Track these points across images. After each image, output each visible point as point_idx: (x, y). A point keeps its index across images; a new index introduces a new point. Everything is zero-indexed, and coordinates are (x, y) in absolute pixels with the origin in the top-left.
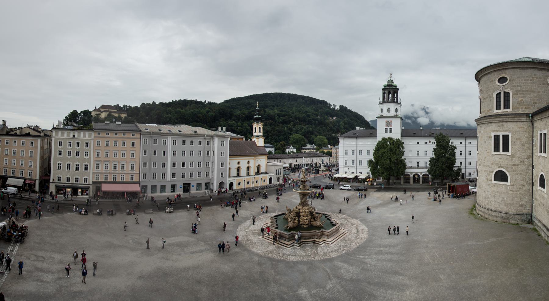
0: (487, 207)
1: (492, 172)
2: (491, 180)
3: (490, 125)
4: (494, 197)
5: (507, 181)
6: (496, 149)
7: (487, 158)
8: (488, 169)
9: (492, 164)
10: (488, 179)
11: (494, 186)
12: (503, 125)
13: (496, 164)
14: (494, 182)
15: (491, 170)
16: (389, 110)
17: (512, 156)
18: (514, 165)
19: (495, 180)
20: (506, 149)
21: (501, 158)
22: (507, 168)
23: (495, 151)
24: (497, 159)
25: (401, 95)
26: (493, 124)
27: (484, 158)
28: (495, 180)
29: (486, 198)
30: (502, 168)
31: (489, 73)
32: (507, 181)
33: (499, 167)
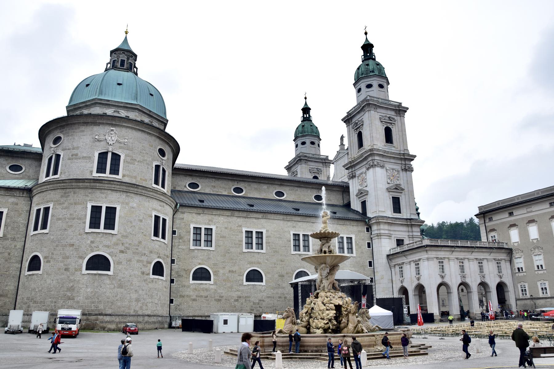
0: (140, 313)
1: (151, 263)
2: (148, 274)
3: (151, 200)
4: (152, 297)
5: (162, 275)
7: (143, 243)
8: (144, 258)
9: (151, 252)
10: (143, 273)
11: (153, 281)
12: (163, 207)
13: (155, 252)
14: (152, 276)
15: (149, 260)
19: (153, 274)
23: (154, 236)
24: (156, 246)
26: (154, 200)
27: (137, 243)
28: (153, 274)
29: (137, 300)
31: (150, 134)
32: (162, 275)
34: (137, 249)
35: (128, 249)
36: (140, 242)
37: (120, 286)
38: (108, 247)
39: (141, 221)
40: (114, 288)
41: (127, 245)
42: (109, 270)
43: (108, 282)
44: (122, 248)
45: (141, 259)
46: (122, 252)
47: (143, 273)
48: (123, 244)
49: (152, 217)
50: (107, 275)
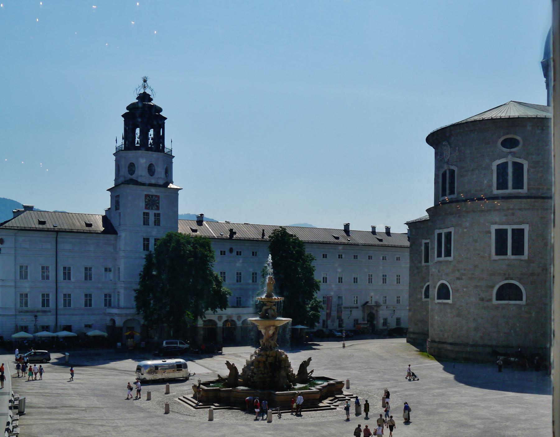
1: (493, 287)
2: (490, 300)
6: (501, 250)
9: (493, 275)
14: (495, 302)
16: (151, 170)
17: (529, 261)
18: (532, 274)
20: (518, 249)
21: (509, 265)
22: (520, 280)
25: (172, 138)
28: (498, 298)
30: (512, 279)
33: (507, 279)
34: (473, 274)
35: (463, 274)
36: (476, 266)
37: (459, 315)
38: (447, 274)
39: (476, 241)
40: (454, 317)
41: (462, 271)
42: (448, 298)
43: (449, 311)
44: (457, 274)
45: (478, 284)
46: (458, 279)
47: (482, 300)
48: (458, 270)
49: (489, 232)
50: (448, 303)
